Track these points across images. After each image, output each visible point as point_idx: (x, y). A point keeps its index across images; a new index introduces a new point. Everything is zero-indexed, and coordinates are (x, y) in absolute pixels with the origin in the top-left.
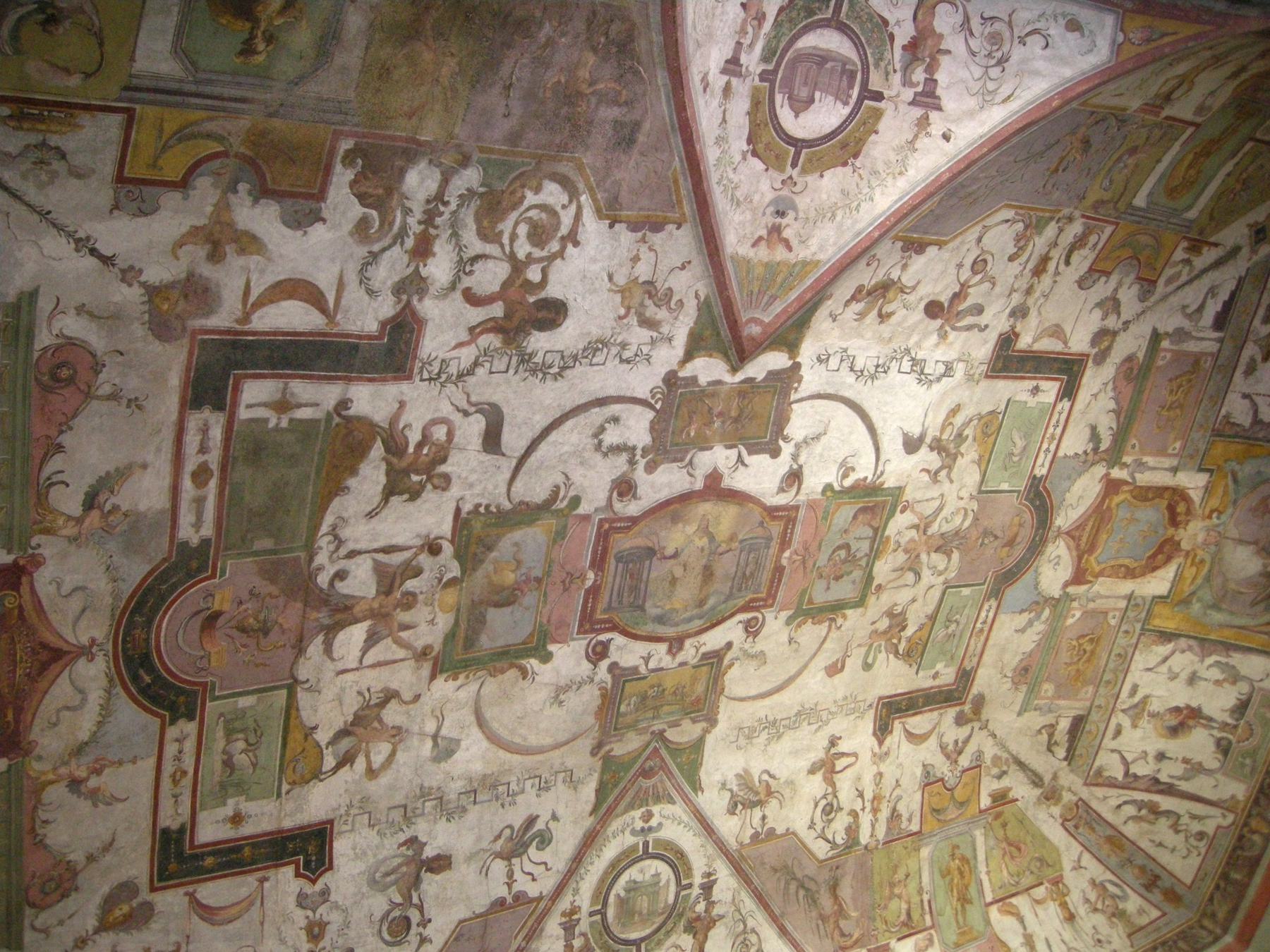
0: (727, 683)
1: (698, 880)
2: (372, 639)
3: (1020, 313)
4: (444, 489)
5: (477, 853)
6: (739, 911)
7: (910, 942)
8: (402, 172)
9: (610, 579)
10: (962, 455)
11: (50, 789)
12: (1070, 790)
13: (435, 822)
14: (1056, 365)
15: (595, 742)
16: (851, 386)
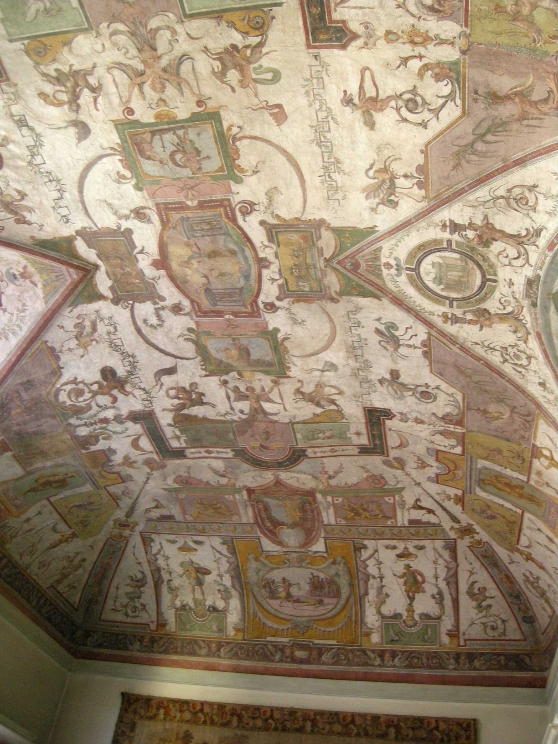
0: (292, 217)
1: (446, 235)
2: (270, 400)
6: (486, 202)
8: (83, 437)
9: (227, 307)
10: (71, 66)
15: (329, 302)
16: (71, 194)
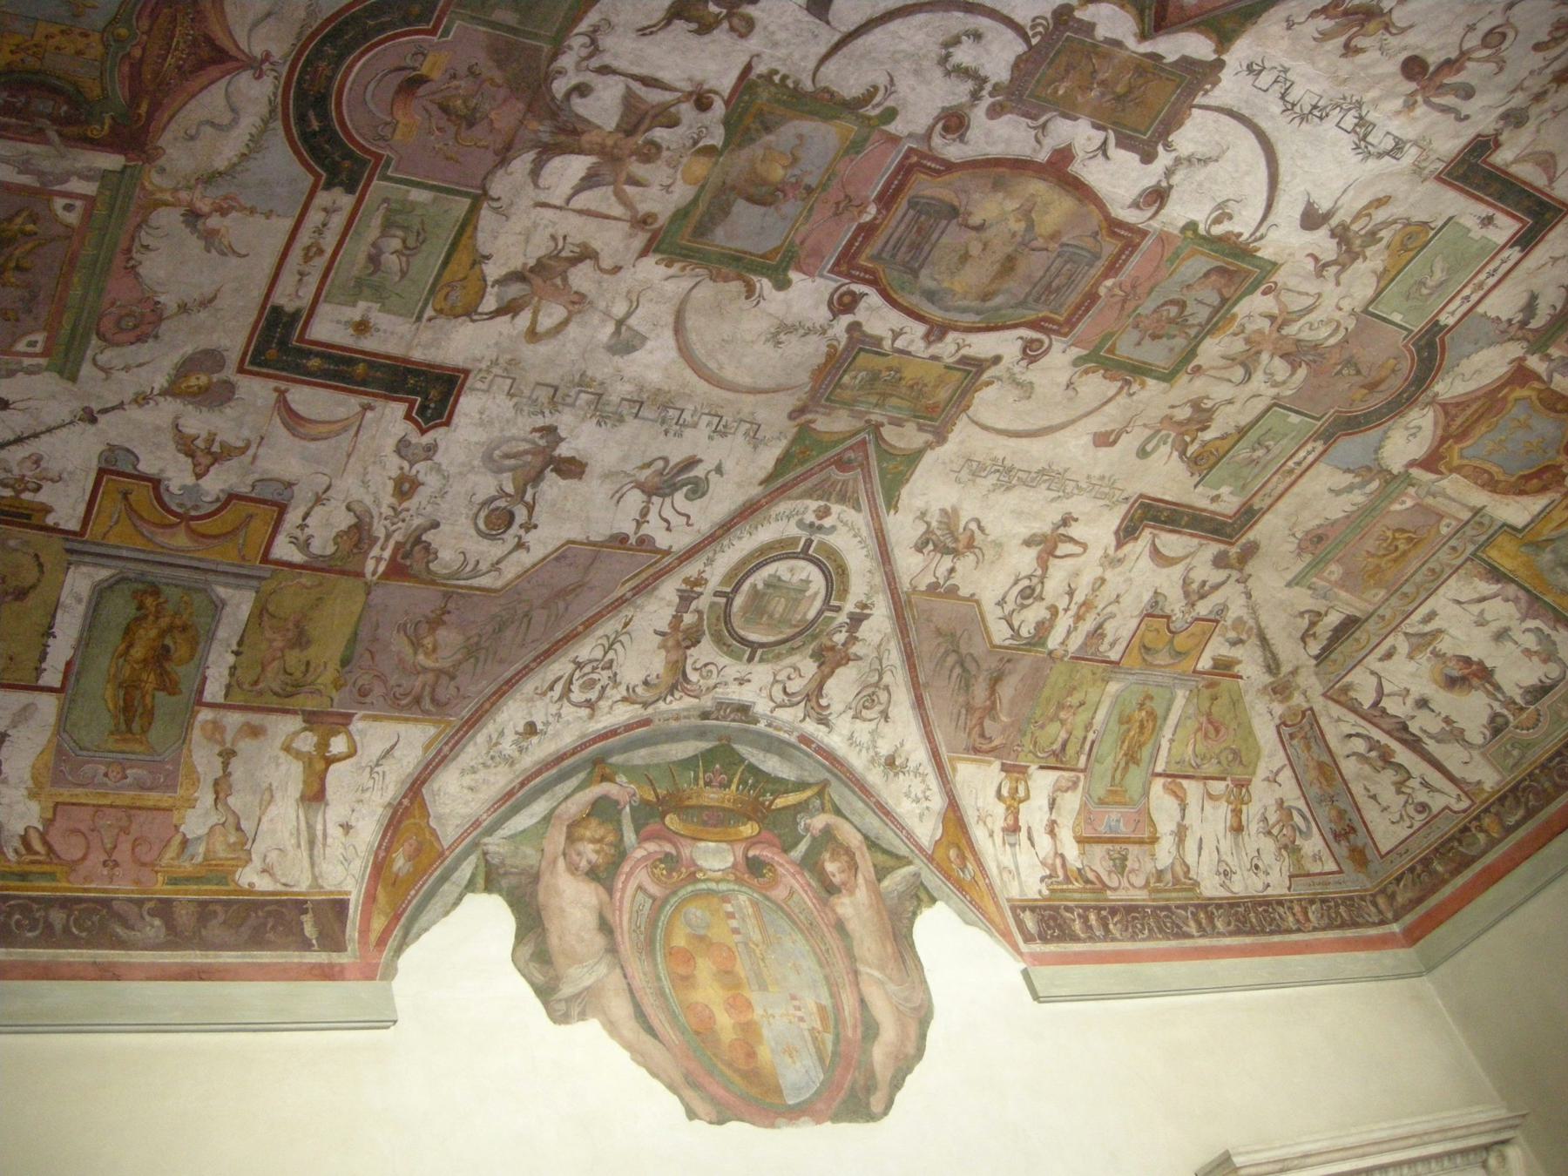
0: (976, 401)
1: (850, 606)
2: (590, 181)
3: (1514, 118)
4: (742, 36)
5: (617, 473)
7: (1052, 776)
9: (893, 223)
10: (1365, 258)
11: (163, 211)
12: (1304, 693)
13: (583, 420)
14: (1526, 203)
15: (799, 404)
16: (1272, 117)
